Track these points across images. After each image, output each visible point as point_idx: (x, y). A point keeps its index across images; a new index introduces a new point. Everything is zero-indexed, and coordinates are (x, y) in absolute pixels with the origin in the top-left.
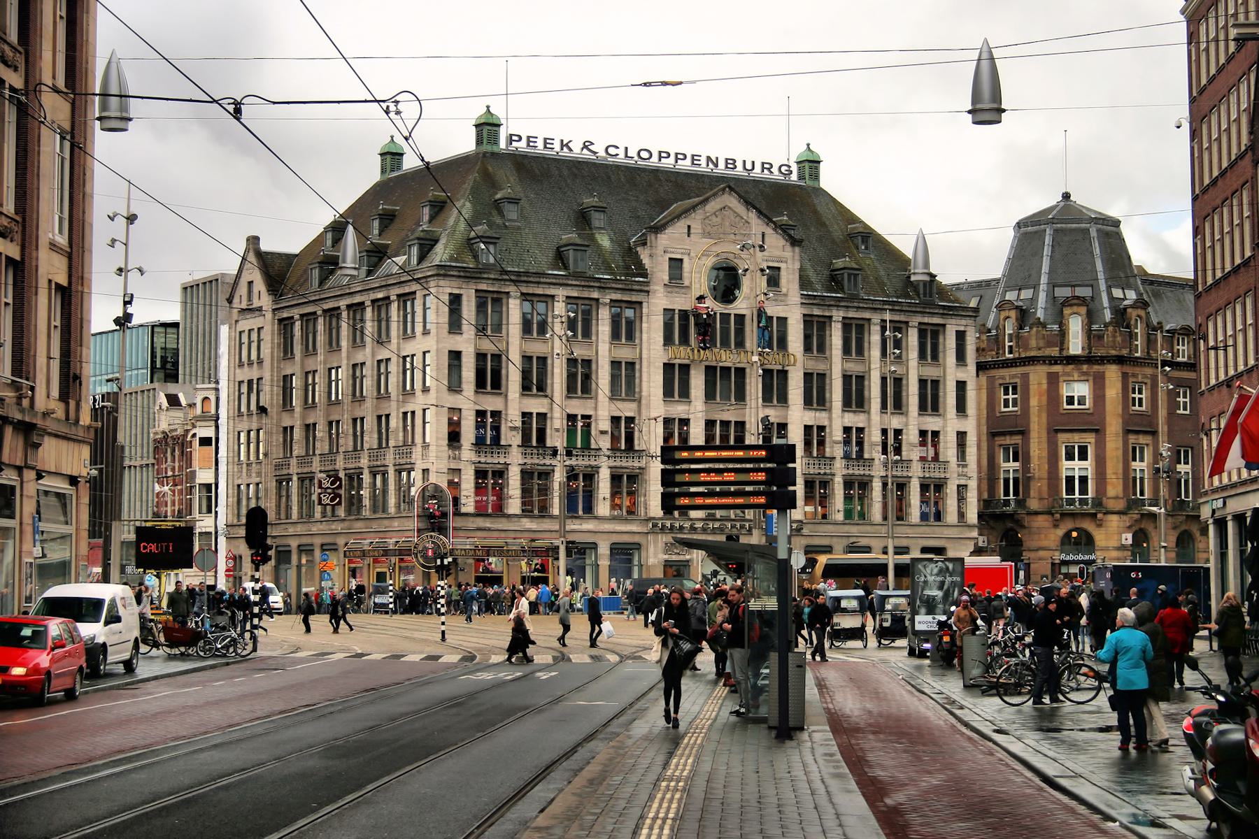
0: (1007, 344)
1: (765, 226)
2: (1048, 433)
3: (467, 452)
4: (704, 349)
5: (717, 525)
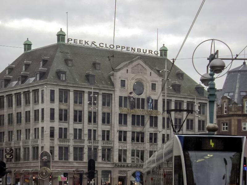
0: (225, 110)
4: (132, 109)
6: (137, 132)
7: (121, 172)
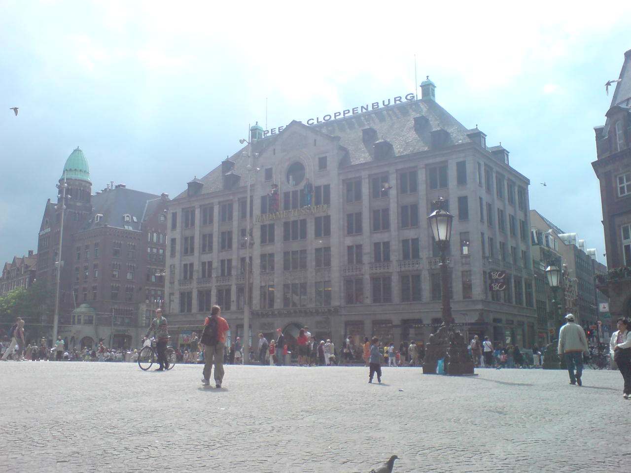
6: (292, 252)
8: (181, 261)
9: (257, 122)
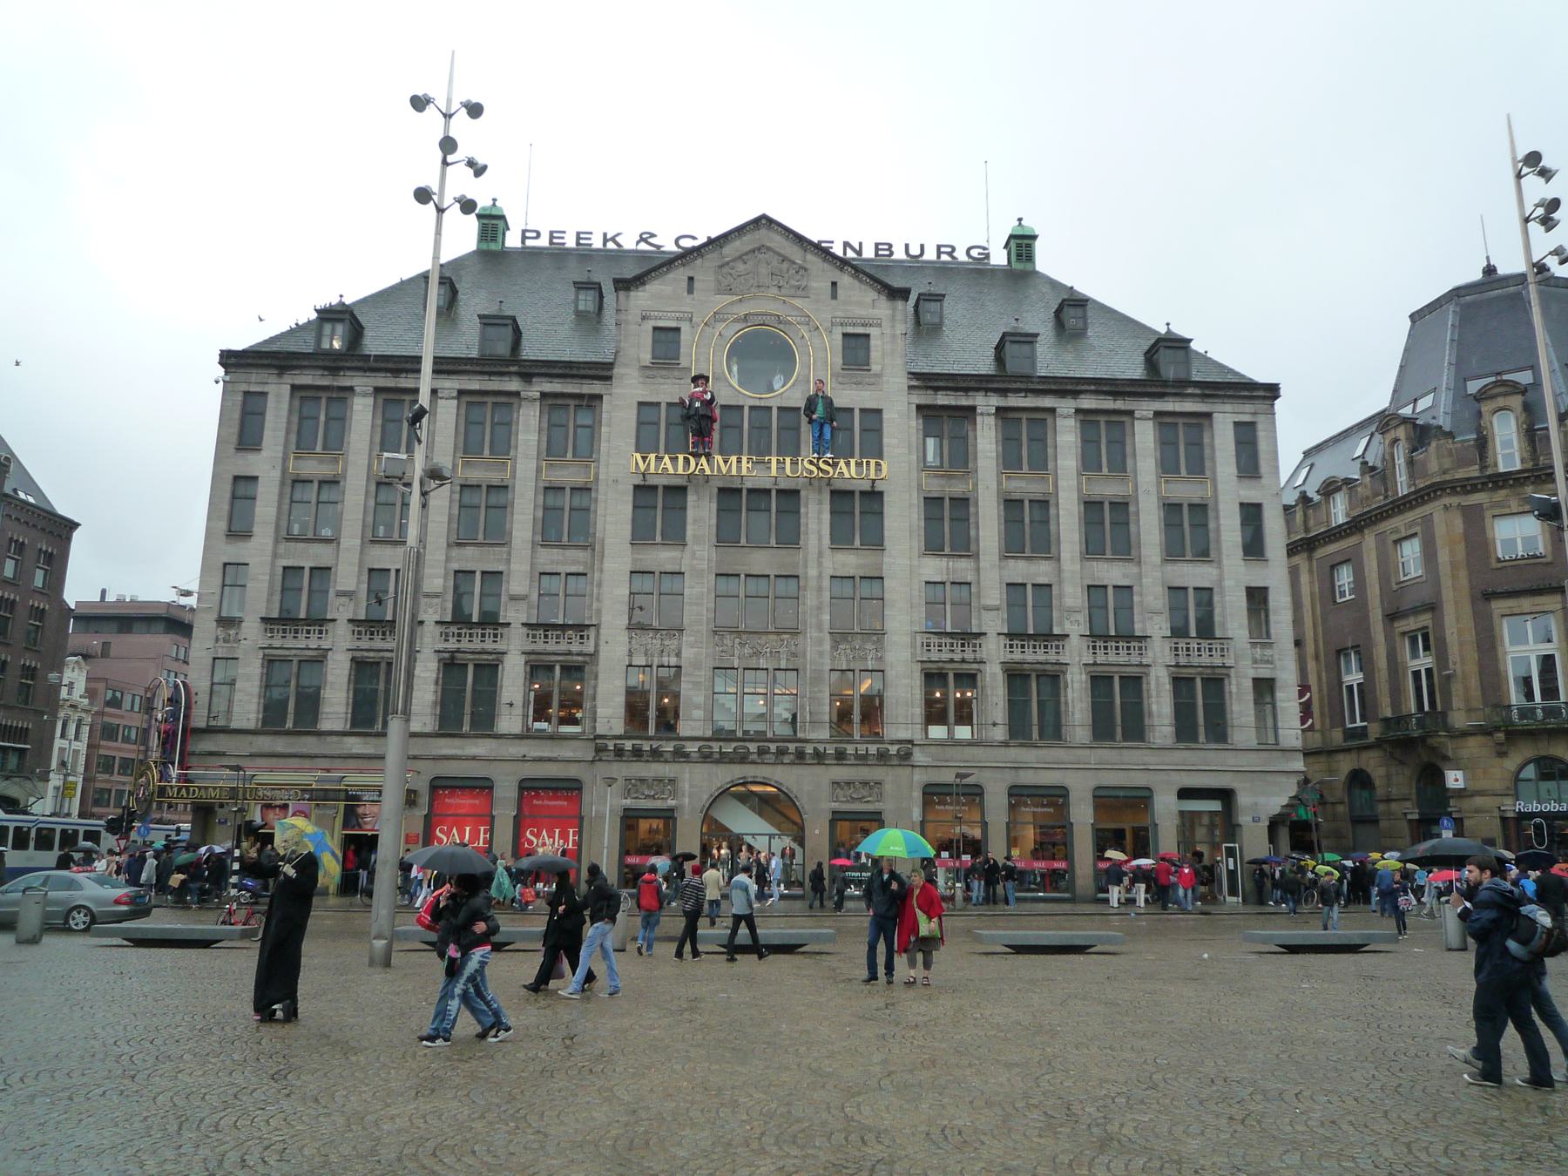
1: (838, 272)
2: (1473, 602)
3: (252, 631)
5: (729, 748)
7: (634, 785)
8: (275, 555)
9: (495, 200)
